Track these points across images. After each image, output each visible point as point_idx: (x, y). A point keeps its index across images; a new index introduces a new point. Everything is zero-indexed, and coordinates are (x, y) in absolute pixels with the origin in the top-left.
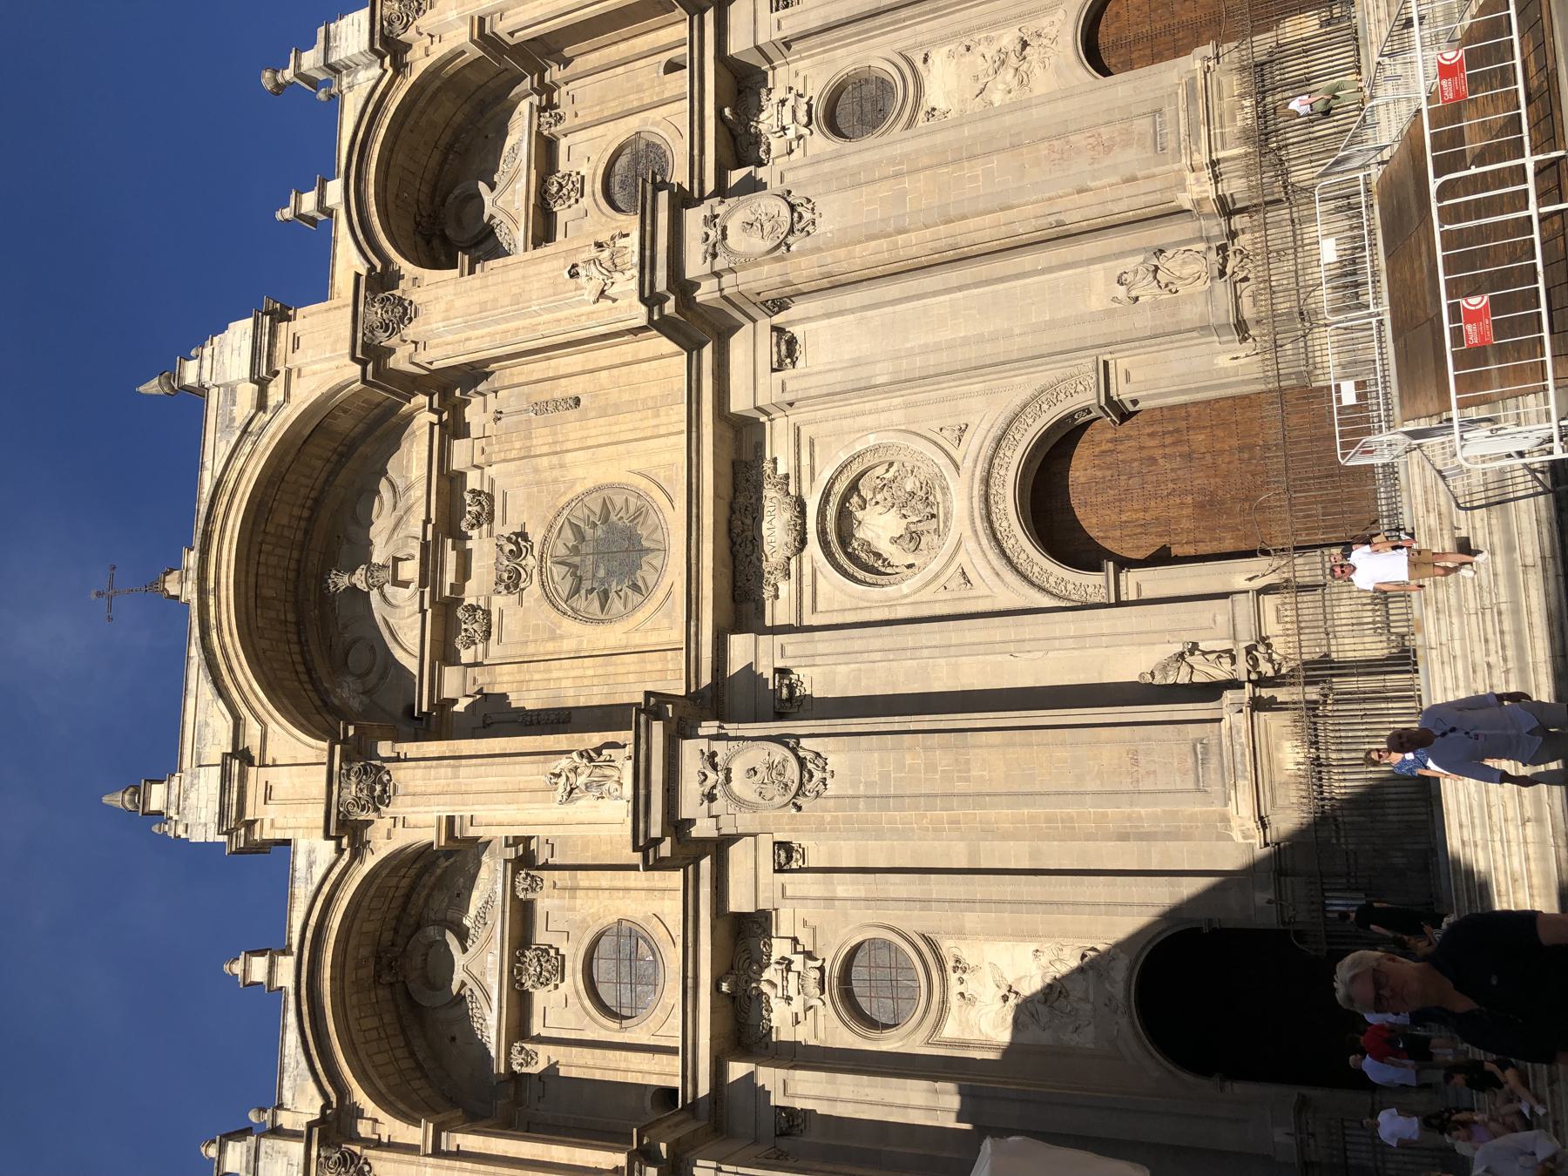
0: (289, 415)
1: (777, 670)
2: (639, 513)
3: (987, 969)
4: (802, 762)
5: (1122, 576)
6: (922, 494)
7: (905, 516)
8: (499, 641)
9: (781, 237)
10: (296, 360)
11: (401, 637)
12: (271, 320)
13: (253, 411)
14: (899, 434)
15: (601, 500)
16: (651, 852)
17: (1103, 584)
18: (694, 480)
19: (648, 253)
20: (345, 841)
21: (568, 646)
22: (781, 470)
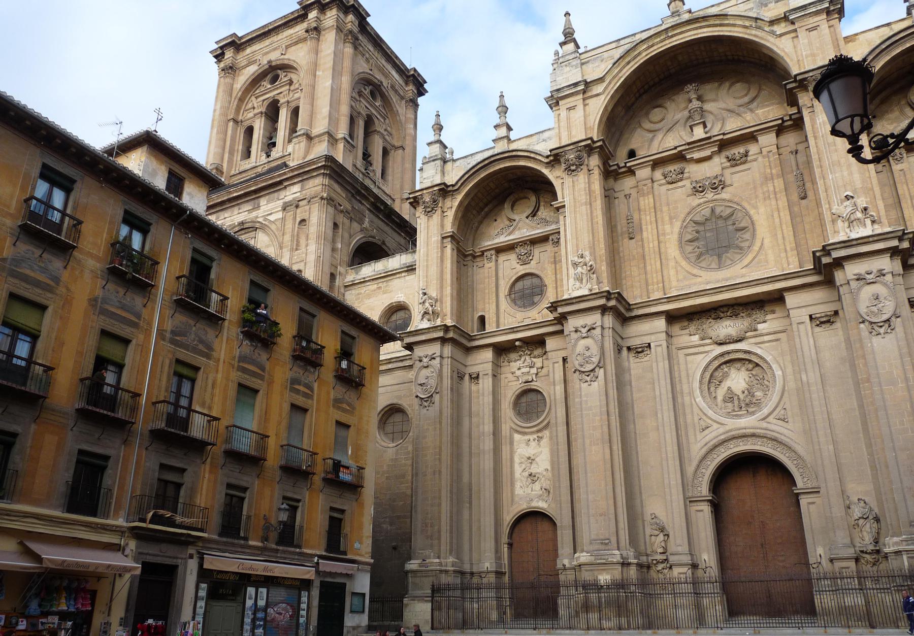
0: (768, 41)
1: (649, 344)
2: (741, 248)
3: (540, 450)
4: (593, 370)
5: (706, 503)
6: (754, 401)
7: (744, 392)
8: (668, 190)
9: (868, 318)
10: (802, 33)
11: (670, 134)
12: (827, 8)
13: (768, 20)
14: (781, 387)
15: (746, 225)
16: (552, 309)
17: (703, 495)
18: (740, 286)
19: (854, 243)
20: (552, 158)
21: (668, 228)
22: (760, 326)
